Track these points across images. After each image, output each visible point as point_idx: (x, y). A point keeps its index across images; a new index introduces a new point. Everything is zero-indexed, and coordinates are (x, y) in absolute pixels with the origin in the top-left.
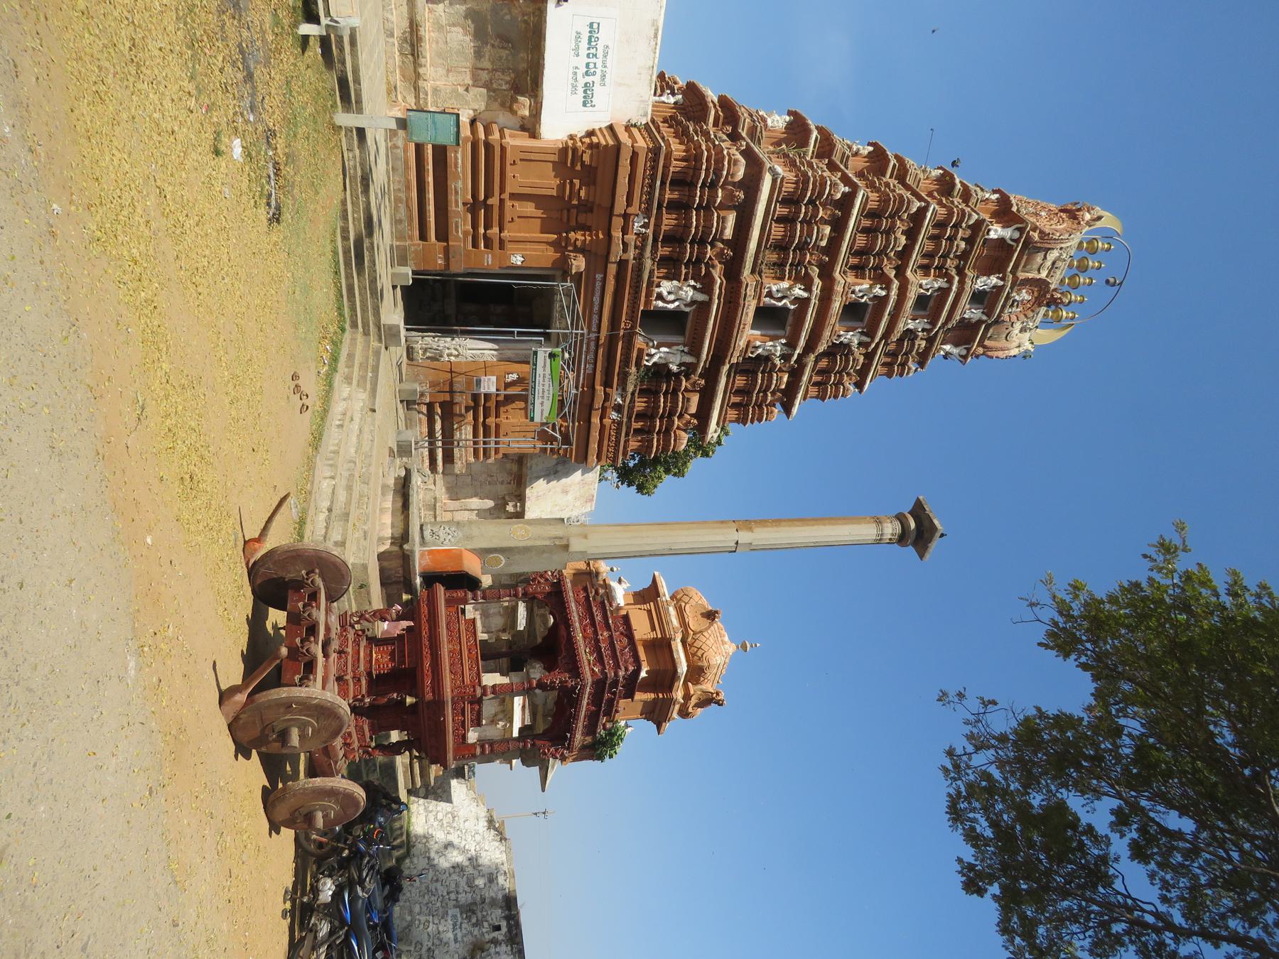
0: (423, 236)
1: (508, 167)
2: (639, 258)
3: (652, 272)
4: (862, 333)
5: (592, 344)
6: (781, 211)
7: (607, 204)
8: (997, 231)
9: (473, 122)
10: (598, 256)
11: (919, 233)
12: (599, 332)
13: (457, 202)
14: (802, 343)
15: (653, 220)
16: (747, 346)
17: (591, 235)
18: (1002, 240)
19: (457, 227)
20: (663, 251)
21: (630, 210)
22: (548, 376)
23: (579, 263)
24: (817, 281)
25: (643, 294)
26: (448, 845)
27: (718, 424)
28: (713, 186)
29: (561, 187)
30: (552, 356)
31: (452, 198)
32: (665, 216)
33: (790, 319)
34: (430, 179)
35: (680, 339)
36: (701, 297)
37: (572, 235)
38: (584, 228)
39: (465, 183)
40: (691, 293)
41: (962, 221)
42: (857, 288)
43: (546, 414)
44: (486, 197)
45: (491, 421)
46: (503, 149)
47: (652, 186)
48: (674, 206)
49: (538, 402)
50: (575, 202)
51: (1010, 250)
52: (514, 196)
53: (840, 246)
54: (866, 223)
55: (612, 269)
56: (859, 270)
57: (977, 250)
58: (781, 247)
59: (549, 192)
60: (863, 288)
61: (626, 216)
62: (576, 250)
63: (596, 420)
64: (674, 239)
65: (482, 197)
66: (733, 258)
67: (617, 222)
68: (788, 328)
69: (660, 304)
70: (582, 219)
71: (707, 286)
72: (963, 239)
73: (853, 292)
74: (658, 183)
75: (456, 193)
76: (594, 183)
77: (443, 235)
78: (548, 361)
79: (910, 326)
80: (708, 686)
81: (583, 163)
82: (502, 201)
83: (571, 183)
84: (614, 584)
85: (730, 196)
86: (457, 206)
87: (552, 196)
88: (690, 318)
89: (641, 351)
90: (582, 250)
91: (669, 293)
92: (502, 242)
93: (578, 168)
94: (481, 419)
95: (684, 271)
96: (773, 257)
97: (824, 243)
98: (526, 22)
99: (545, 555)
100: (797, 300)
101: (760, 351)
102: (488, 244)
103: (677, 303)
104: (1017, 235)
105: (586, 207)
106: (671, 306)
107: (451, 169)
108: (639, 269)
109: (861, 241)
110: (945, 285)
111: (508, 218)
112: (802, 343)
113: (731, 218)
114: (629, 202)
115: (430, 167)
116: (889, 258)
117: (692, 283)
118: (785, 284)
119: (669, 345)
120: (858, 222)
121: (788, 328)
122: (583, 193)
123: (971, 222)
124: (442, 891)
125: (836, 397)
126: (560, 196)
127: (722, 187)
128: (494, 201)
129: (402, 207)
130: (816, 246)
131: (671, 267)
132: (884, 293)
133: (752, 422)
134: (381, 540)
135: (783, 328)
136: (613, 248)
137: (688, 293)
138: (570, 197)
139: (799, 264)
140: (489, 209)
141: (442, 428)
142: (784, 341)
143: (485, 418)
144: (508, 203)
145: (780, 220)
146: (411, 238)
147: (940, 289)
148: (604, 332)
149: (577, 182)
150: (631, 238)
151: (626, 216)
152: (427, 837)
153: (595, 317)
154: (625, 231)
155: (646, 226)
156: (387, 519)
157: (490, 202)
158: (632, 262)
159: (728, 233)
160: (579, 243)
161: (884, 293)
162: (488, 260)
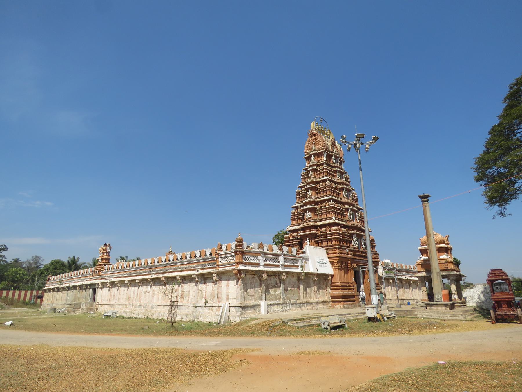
0: (354, 301)
9: (331, 289)
18: (326, 157)
23: (355, 265)
24: (347, 207)
26: (479, 298)
37: (349, 266)
46: (341, 283)
56: (339, 194)
80: (446, 239)
84: (422, 259)
90: (351, 264)
124: (489, 300)
134: (446, 309)
150: (349, 253)
152: (477, 303)
156: (440, 308)
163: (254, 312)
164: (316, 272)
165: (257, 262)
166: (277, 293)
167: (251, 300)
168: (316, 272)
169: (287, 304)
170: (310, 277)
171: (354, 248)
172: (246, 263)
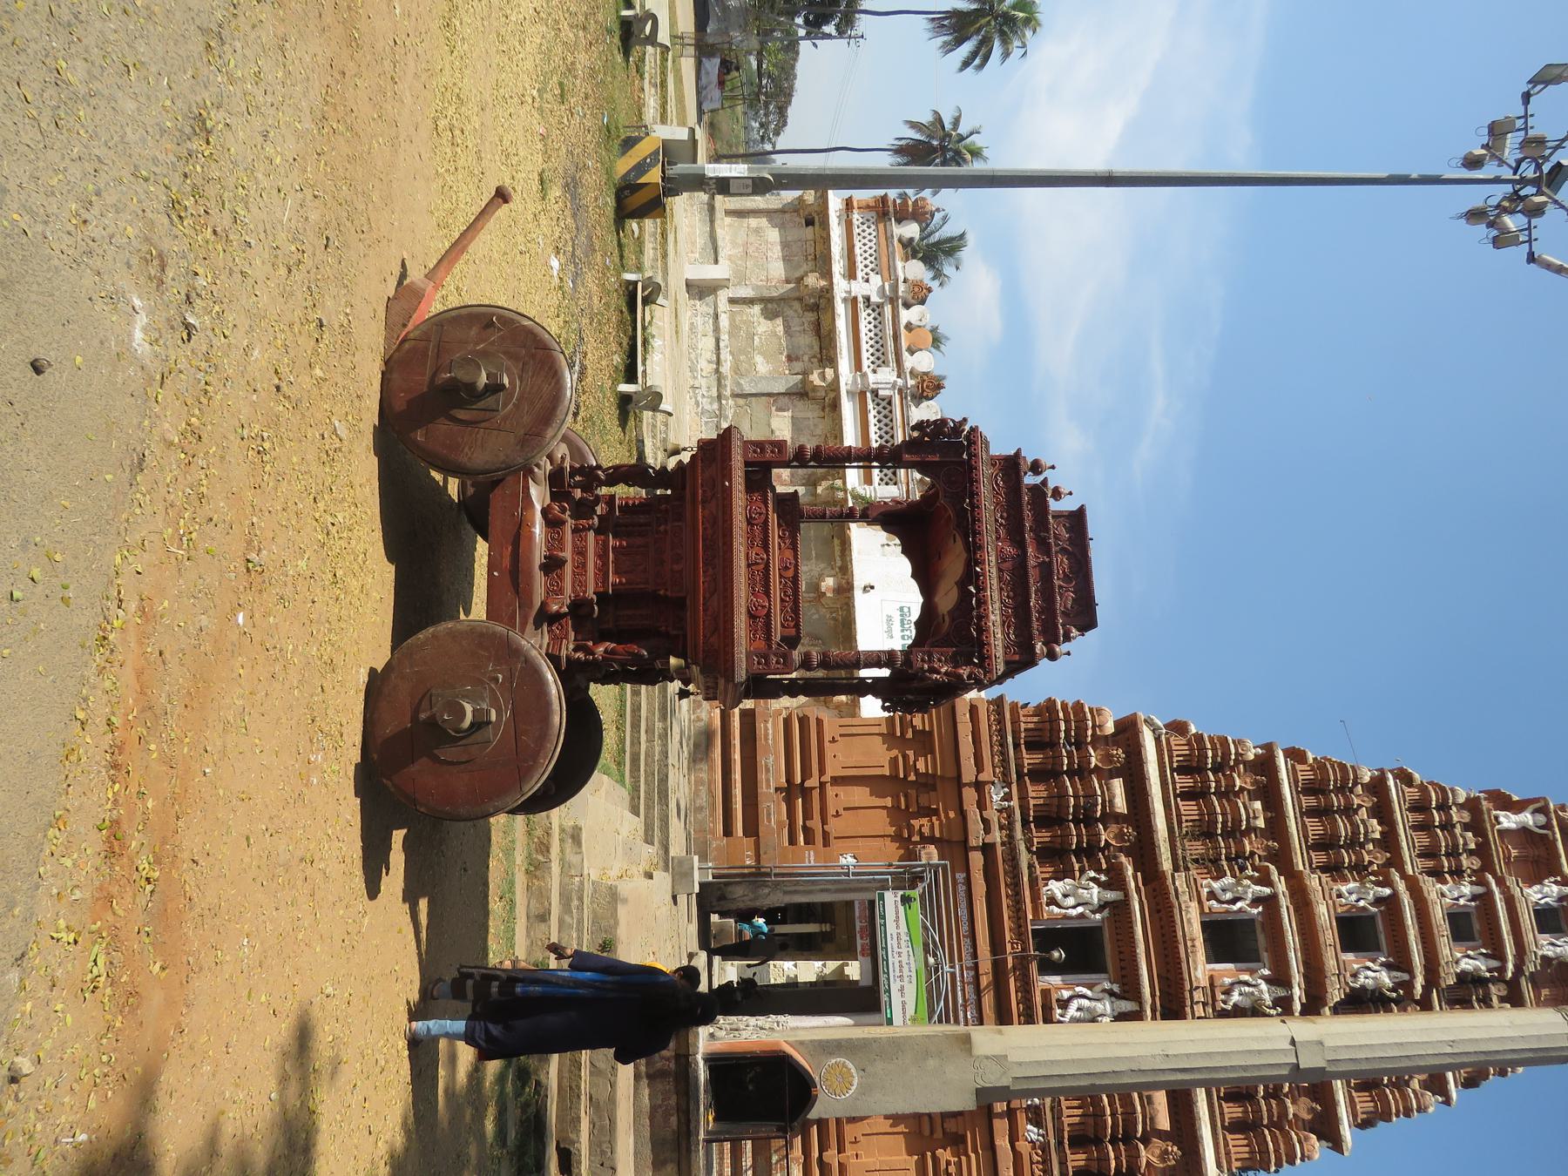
0: (728, 831)
1: (827, 744)
2: (1010, 842)
3: (1031, 866)
4: (1388, 966)
5: (969, 989)
6: (1183, 782)
7: (951, 773)
8: (1509, 821)
10: (955, 846)
11: (1392, 812)
12: (975, 955)
13: (768, 781)
14: (1297, 978)
15: (1014, 787)
16: (1212, 985)
17: (939, 818)
18: (1524, 830)
19: (769, 814)
20: (1041, 837)
21: (982, 777)
22: (904, 938)
23: (930, 854)
25: (1027, 893)
27: (1219, 1166)
28: (1080, 744)
29: (894, 761)
30: (906, 900)
31: (762, 776)
32: (1030, 788)
33: (1262, 940)
34: (737, 756)
35: (1103, 976)
36: (1111, 895)
37: (916, 823)
38: (929, 812)
39: (777, 759)
40: (1095, 890)
41: (1446, 798)
42: (1344, 889)
43: (910, 1011)
44: (803, 781)
45: (832, 1156)
47: (1003, 744)
48: (1038, 775)
49: (895, 987)
50: (912, 777)
51: (1549, 844)
52: (836, 781)
53: (1285, 828)
54: (1309, 801)
55: (977, 859)
56: (1334, 870)
57: (1497, 850)
58: (1205, 831)
59: (878, 772)
60: (1354, 893)
61: (979, 786)
62: (927, 840)
63: (1002, 1142)
64: (1049, 818)
65: (798, 780)
66: (1139, 839)
67: (970, 795)
68: (1265, 956)
69: (1056, 910)
70: (924, 801)
71: (1115, 880)
72: (1466, 827)
73: (1339, 896)
74: (1010, 739)
75: (768, 770)
76: (932, 752)
77: (752, 829)
78: (901, 909)
79: (1467, 965)
81: (914, 727)
82: (822, 785)
83: (905, 757)
85: (1108, 758)
86: (768, 786)
87: (883, 776)
88: (1106, 935)
89: (1046, 994)
90: (931, 840)
91: (1065, 896)
92: (825, 835)
93: (910, 735)
94: (816, 1154)
95: (1077, 866)
96: (1196, 848)
97: (1261, 823)
98: (835, 619)
99: (932, 1063)
100: (1256, 901)
101: (1235, 997)
102: (809, 840)
103: (1080, 909)
104: (1542, 819)
105: (927, 783)
106: (1074, 912)
107: (760, 743)
108: (1012, 859)
109: (1315, 827)
110: (1479, 890)
111: (831, 811)
112: (1297, 978)
113: (1118, 785)
114: (979, 766)
115: (737, 742)
116: (1369, 852)
117: (1092, 874)
118: (1228, 880)
119: (1090, 987)
120: (1297, 803)
121: (1265, 956)
122: (921, 766)
123: (1461, 800)
125: (1408, 1112)
126: (894, 777)
127: (1094, 743)
128: (812, 782)
129: (703, 790)
130: (1251, 829)
131: (1057, 859)
132: (1387, 891)
133: (1279, 1165)
135: (1258, 959)
136: (971, 826)
137: (1094, 894)
138: (906, 776)
139: (1237, 857)
140: (806, 793)
141: (754, 1166)
142: (1266, 972)
143: (823, 1148)
144: (831, 791)
145: (1187, 795)
146: (713, 832)
147: (1474, 898)
148: (986, 965)
149: (911, 753)
151: (979, 786)
153: (966, 943)
154: (981, 805)
155: (1007, 797)
157: (808, 784)
158: (999, 849)
159: (1121, 804)
160: (926, 831)
161: (1387, 891)
162: (810, 859)
163: (694, 243)
164: (858, 583)
165: (860, 274)
166: (759, 359)
167: (734, 244)
168: (860, 578)
169: (719, 397)
170: (830, 560)
171: (1033, 882)
172: (849, 225)
